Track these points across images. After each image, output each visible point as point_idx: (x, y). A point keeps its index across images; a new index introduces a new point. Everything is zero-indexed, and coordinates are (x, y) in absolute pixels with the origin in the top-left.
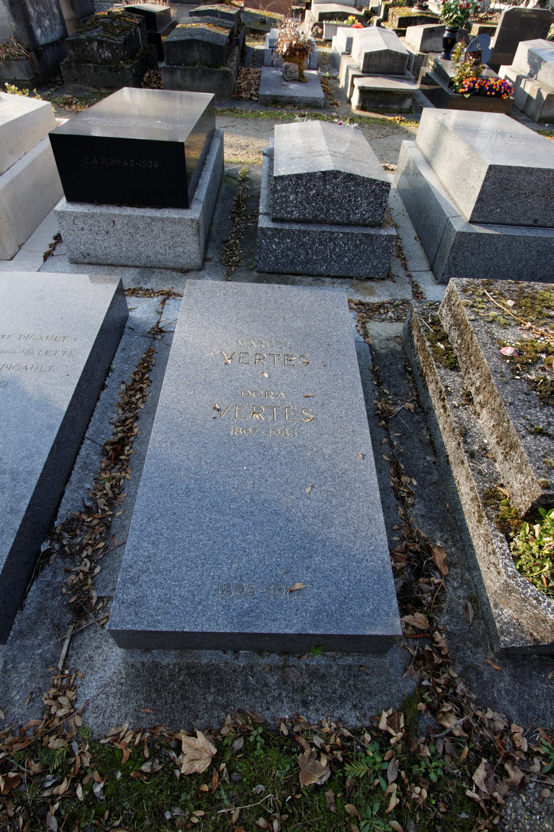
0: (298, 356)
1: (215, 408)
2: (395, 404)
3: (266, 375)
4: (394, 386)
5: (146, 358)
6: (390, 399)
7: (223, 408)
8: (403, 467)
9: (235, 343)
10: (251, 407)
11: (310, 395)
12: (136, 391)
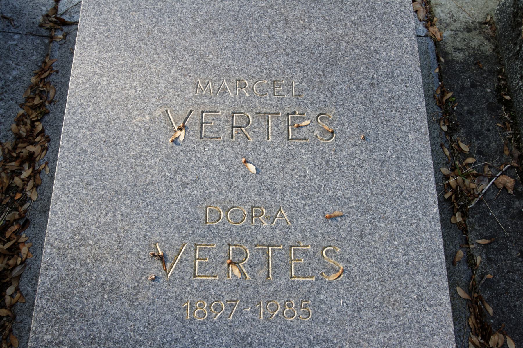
0: (313, 115)
1: (154, 255)
2: (480, 175)
3: (252, 168)
4: (479, 135)
5: (37, 85)
6: (470, 165)
7: (170, 255)
8: (491, 311)
9: (191, 88)
10: (225, 248)
11: (337, 213)
12: (22, 163)
